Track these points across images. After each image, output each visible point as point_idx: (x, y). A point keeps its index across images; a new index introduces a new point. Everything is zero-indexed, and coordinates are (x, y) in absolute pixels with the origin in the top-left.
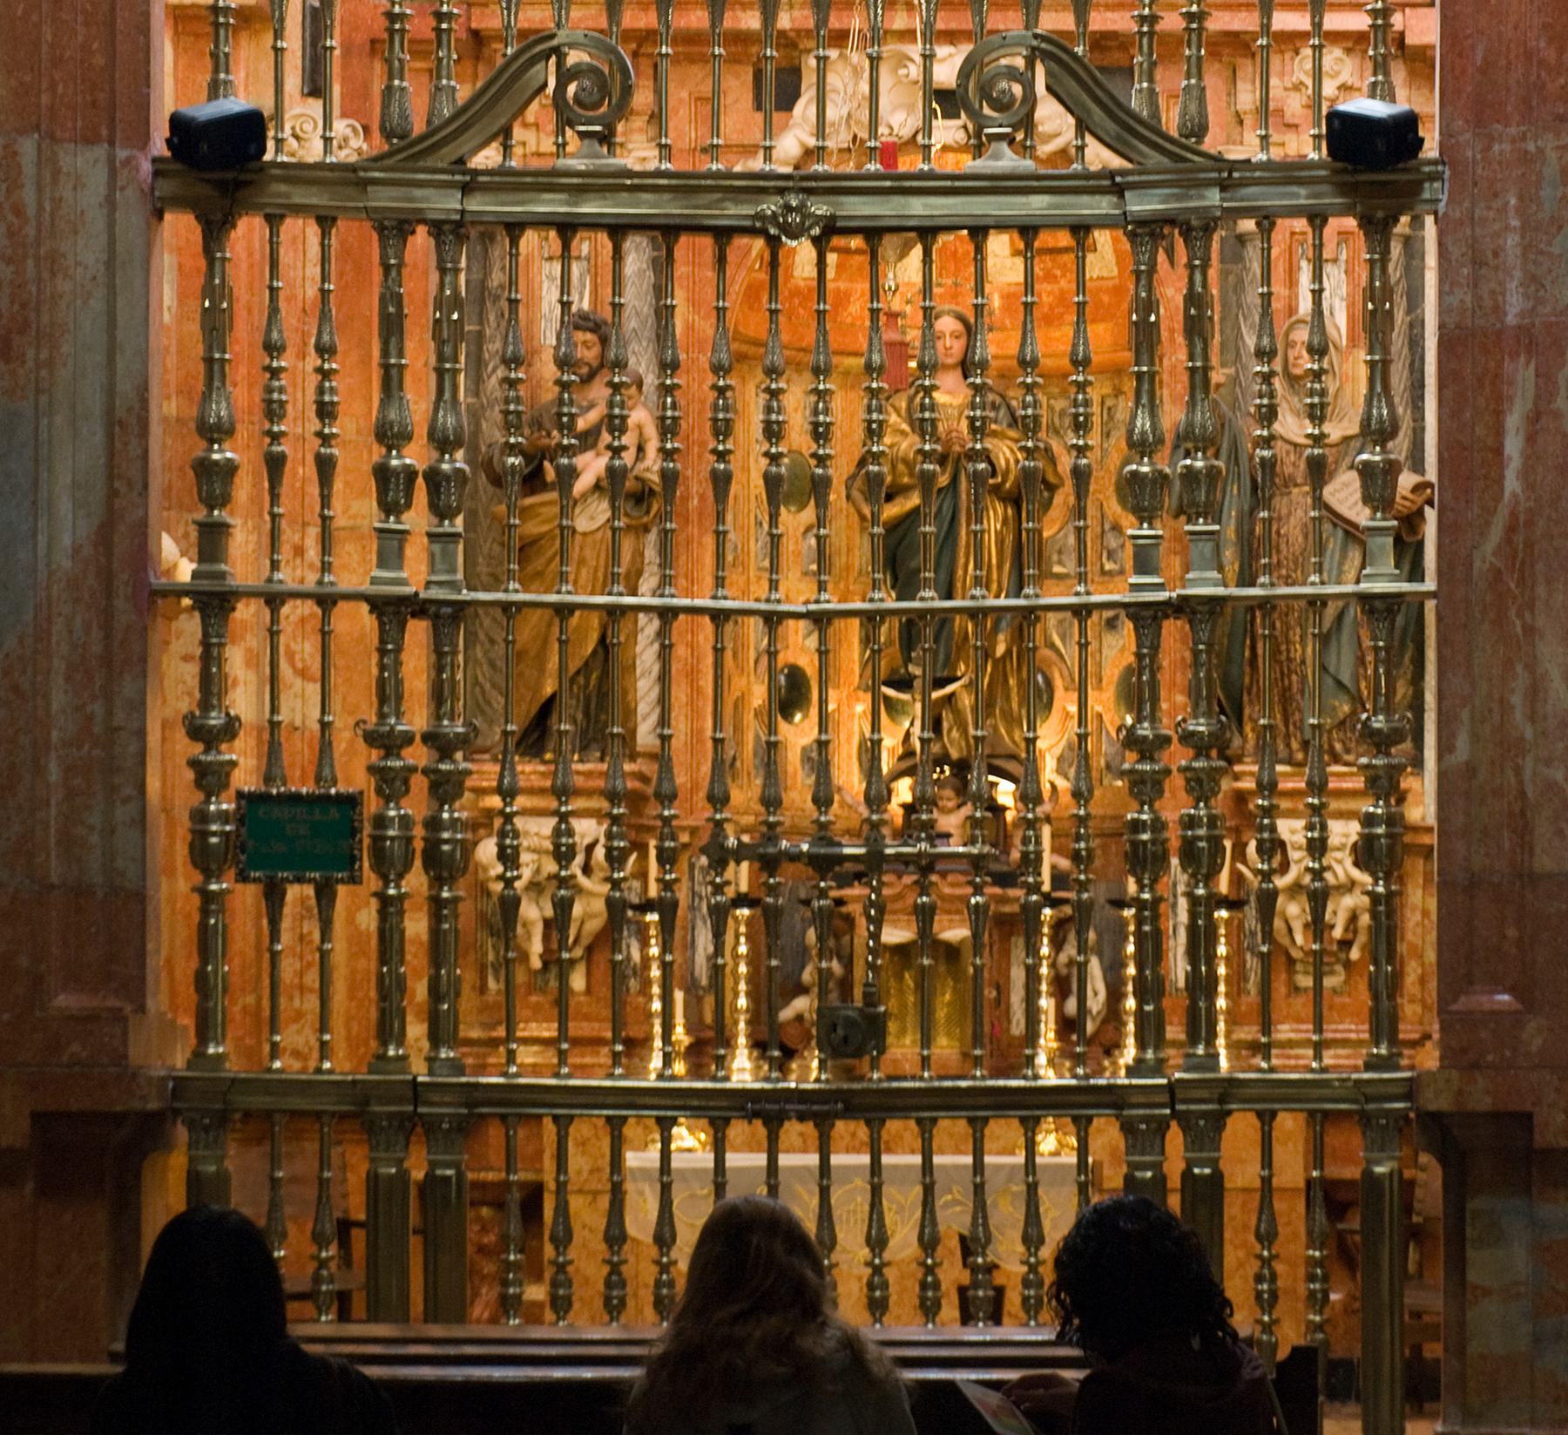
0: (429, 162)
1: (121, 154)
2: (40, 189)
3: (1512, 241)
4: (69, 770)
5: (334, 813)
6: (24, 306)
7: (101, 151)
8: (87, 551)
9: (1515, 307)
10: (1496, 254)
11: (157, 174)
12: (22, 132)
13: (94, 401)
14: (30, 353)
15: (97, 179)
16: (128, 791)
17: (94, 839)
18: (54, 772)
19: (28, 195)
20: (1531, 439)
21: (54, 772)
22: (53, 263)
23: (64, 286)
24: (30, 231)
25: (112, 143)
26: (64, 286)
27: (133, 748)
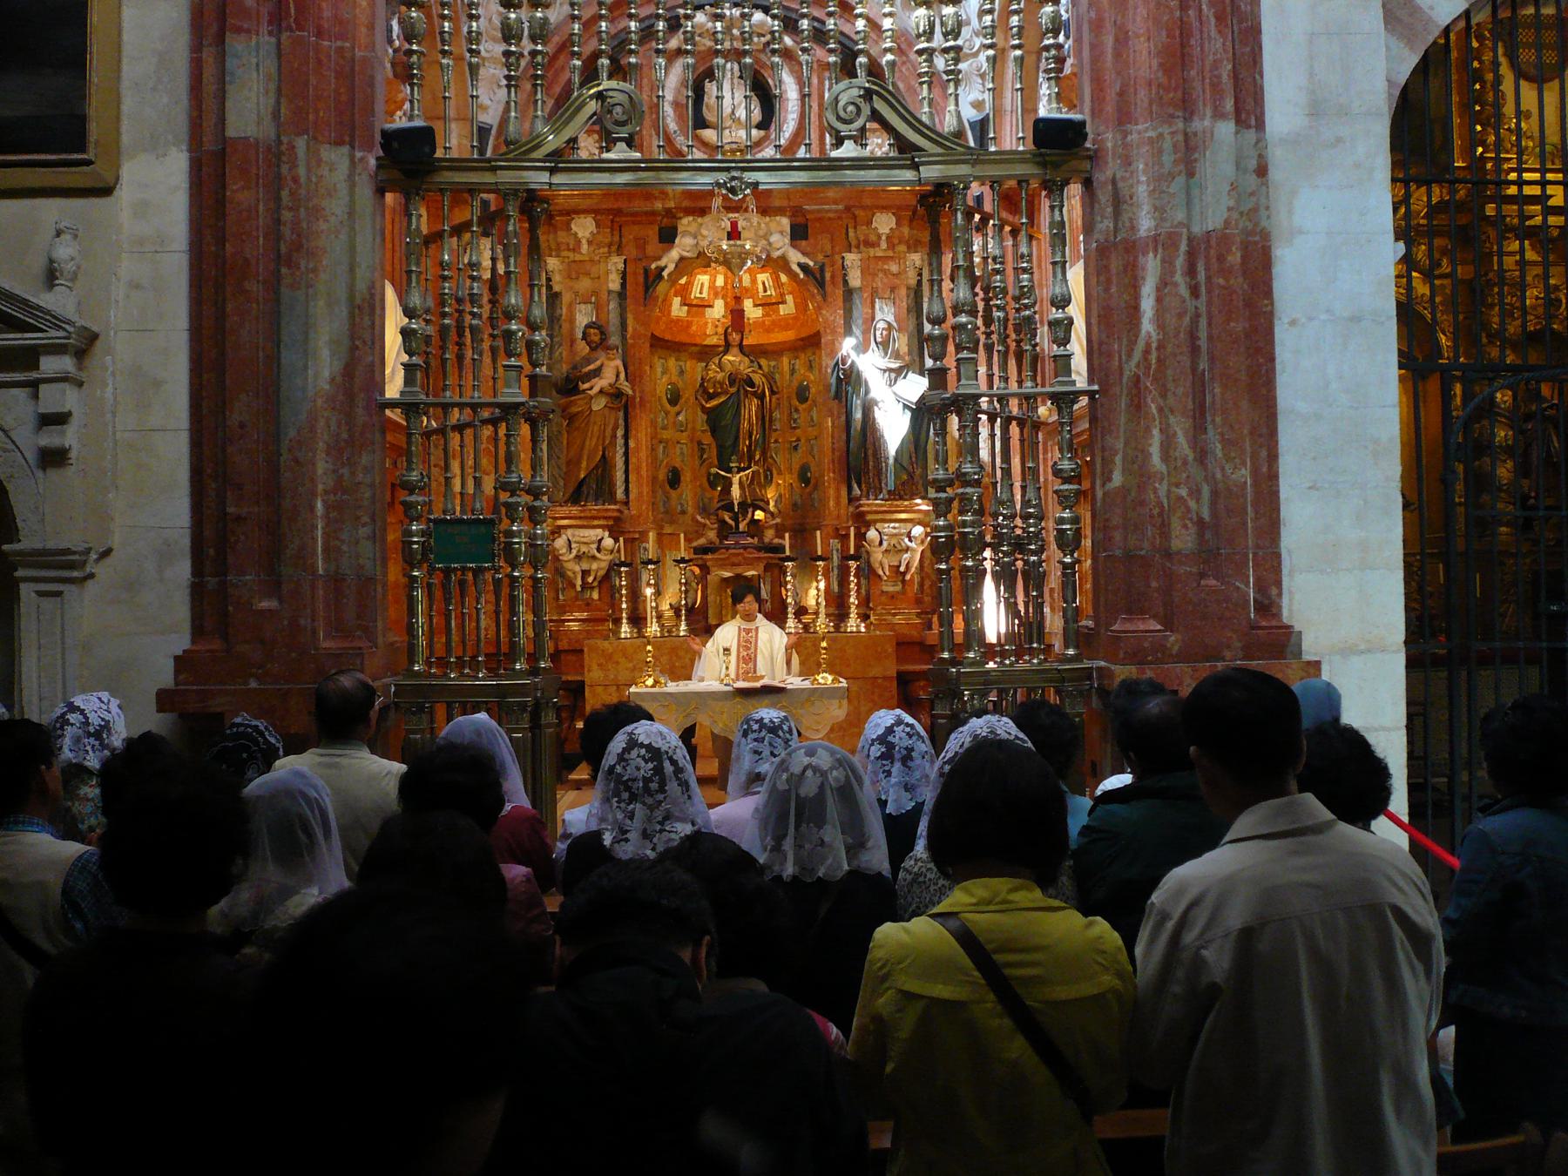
0: (535, 155)
1: (359, 155)
2: (309, 170)
5: (483, 529)
6: (299, 236)
7: (345, 149)
8: (339, 379)
9: (1145, 224)
10: (1131, 198)
11: (379, 167)
12: (299, 134)
13: (342, 294)
14: (303, 263)
15: (343, 167)
16: (366, 519)
18: (319, 505)
19: (302, 171)
20: (1159, 300)
22: (317, 212)
23: (323, 226)
24: (303, 192)
25: (353, 148)
26: (323, 226)
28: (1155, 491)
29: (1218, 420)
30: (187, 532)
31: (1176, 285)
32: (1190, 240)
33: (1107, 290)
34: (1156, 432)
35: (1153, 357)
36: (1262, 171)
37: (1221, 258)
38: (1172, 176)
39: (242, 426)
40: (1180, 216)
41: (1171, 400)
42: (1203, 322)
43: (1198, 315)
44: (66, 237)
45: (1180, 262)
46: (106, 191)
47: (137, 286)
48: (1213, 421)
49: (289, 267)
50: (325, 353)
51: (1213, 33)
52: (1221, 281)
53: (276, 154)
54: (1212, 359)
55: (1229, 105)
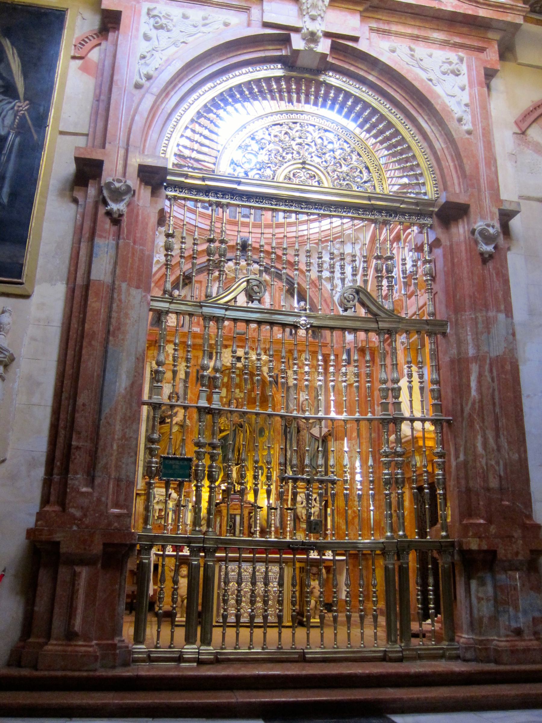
3: (469, 338)
4: (118, 446)
5: (186, 463)
9: (471, 352)
17: (124, 466)
18: (115, 447)
21: (115, 447)
22: (127, 314)
23: (128, 321)
26: (128, 321)
27: (134, 443)
28: (480, 462)
29: (505, 433)
30: (45, 455)
31: (486, 376)
32: (490, 359)
33: (455, 378)
34: (479, 437)
35: (477, 406)
36: (514, 334)
37: (503, 367)
38: (482, 333)
39: (84, 405)
40: (486, 349)
41: (486, 424)
42: (496, 393)
43: (494, 390)
44: (7, 314)
45: (487, 367)
46: (27, 296)
47: (35, 340)
48: (503, 434)
49: (114, 337)
50: (124, 377)
51: (495, 279)
52: (504, 376)
53: (112, 288)
54: (501, 407)
55: (502, 307)
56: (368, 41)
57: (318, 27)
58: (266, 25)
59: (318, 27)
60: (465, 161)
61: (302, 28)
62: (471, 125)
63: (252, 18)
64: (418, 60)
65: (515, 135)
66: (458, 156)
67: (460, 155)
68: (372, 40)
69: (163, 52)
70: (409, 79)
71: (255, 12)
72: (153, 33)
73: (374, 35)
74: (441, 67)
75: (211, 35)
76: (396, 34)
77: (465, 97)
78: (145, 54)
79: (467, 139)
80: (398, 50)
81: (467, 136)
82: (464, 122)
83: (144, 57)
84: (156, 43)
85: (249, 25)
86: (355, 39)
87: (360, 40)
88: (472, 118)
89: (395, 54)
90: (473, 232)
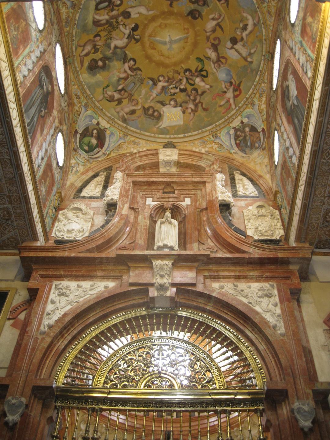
56: (203, 285)
57: (166, 281)
58: (132, 284)
59: (166, 281)
60: (280, 357)
61: (156, 283)
62: (284, 329)
63: (123, 282)
64: (240, 291)
65: (326, 331)
66: (275, 354)
67: (276, 352)
68: (206, 284)
69: (62, 310)
70: (233, 305)
71: (125, 277)
72: (57, 299)
73: (208, 281)
74: (257, 293)
75: (95, 296)
76: (224, 277)
77: (278, 311)
78: (50, 312)
79: (282, 340)
80: (226, 287)
81: (282, 338)
82: (278, 328)
83: (49, 314)
84: (58, 305)
85: (121, 286)
86: (194, 285)
87: (198, 285)
88: (284, 325)
89: (224, 290)
90: (292, 411)
